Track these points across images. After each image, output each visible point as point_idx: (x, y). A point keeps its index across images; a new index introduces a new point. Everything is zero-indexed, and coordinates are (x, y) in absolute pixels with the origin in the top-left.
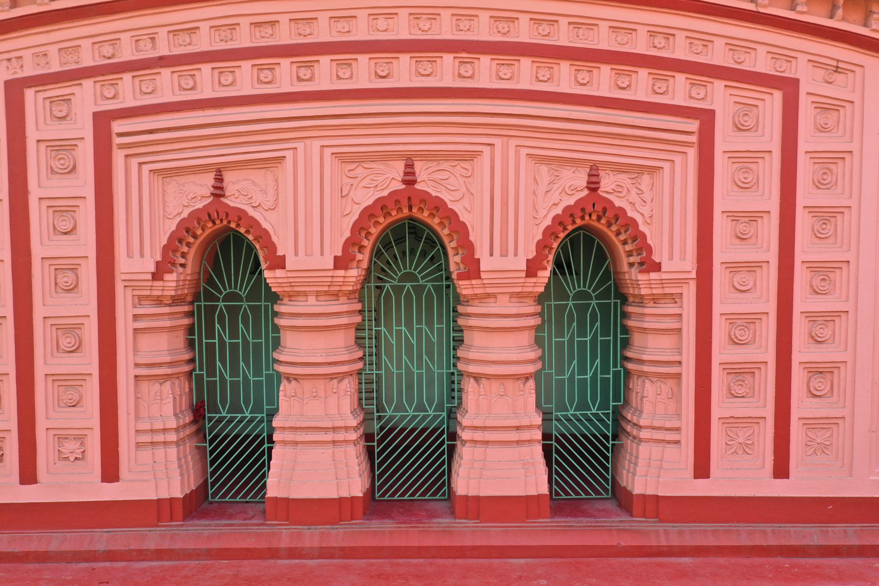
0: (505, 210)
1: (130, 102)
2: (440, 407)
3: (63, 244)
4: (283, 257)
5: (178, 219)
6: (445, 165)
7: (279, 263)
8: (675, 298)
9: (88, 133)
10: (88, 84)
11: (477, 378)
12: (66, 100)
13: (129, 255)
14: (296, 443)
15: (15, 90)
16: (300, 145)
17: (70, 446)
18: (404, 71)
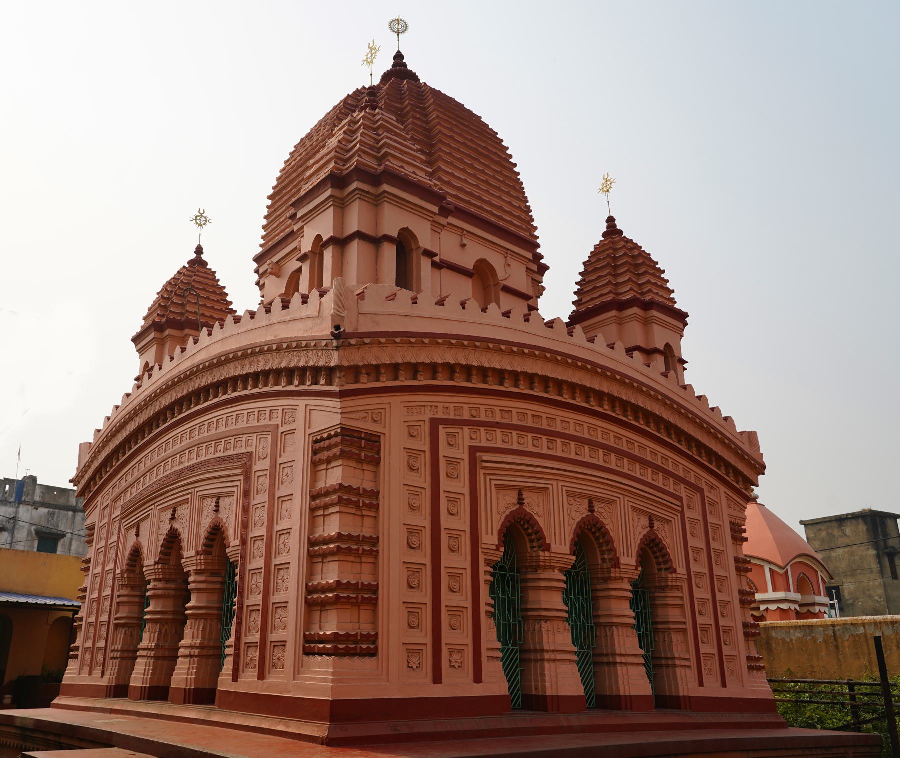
0: (626, 532)
1: (484, 444)
2: (589, 649)
3: (456, 522)
4: (550, 545)
5: (504, 516)
6: (603, 505)
7: (548, 548)
8: (679, 588)
9: (466, 457)
10: (466, 429)
11: (617, 625)
12: (454, 435)
13: (487, 534)
14: (555, 661)
15: (435, 424)
16: (555, 483)
17: (456, 657)
18: (586, 455)
